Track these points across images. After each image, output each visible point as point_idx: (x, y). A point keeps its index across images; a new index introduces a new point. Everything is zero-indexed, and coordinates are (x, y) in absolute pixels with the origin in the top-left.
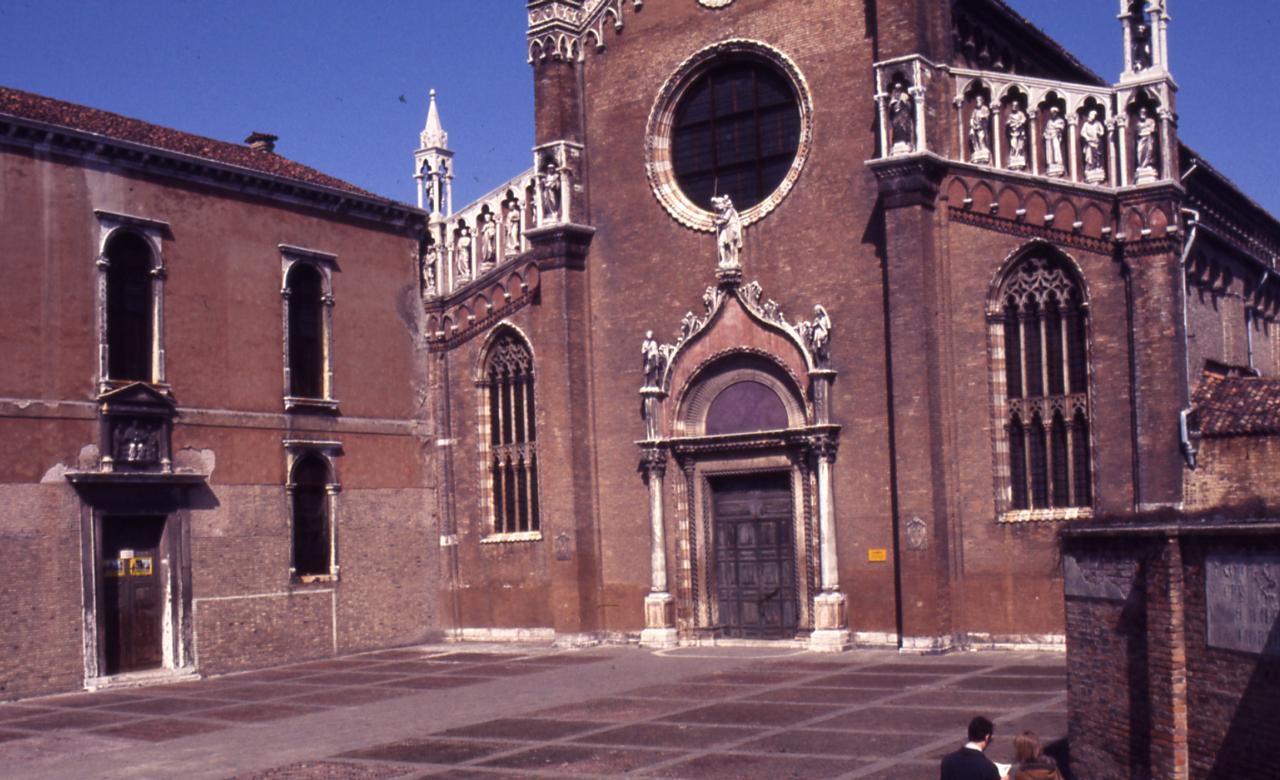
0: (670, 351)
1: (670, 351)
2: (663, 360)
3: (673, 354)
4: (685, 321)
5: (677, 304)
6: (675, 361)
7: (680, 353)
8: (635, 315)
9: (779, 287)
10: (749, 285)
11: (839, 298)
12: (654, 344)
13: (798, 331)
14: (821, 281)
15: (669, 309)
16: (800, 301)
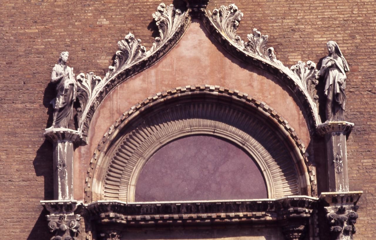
0: (94, 83)
1: (94, 83)
2: (83, 95)
3: (100, 87)
4: (122, 44)
5: (105, 22)
6: (101, 97)
7: (109, 87)
8: (34, 30)
9: (265, 16)
10: (224, 8)
11: (353, 37)
12: (70, 70)
13: (298, 72)
14: (327, 14)
15: (91, 28)
16: (297, 36)
